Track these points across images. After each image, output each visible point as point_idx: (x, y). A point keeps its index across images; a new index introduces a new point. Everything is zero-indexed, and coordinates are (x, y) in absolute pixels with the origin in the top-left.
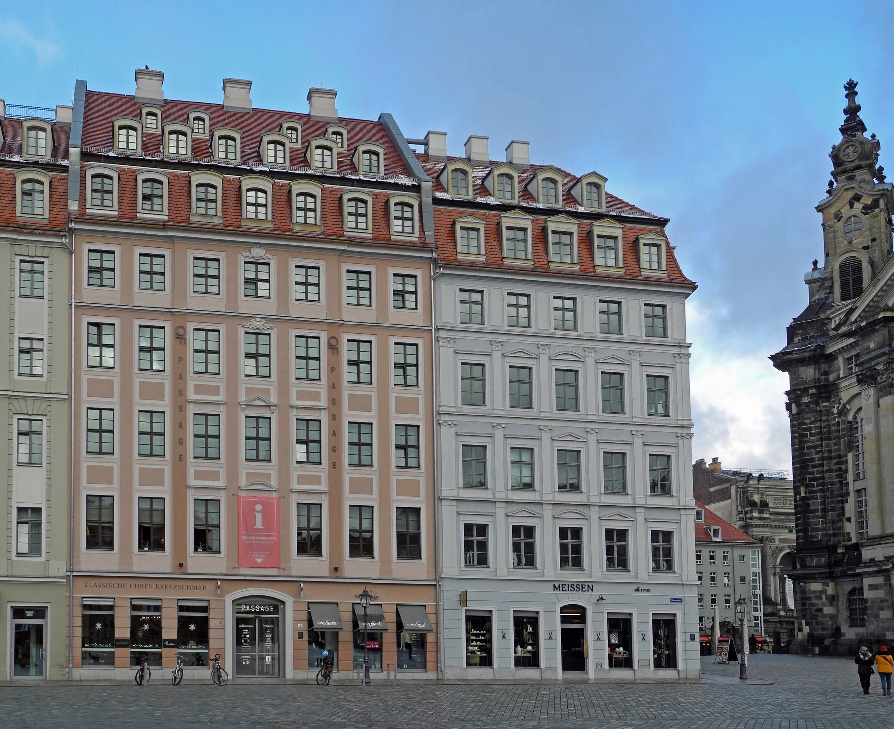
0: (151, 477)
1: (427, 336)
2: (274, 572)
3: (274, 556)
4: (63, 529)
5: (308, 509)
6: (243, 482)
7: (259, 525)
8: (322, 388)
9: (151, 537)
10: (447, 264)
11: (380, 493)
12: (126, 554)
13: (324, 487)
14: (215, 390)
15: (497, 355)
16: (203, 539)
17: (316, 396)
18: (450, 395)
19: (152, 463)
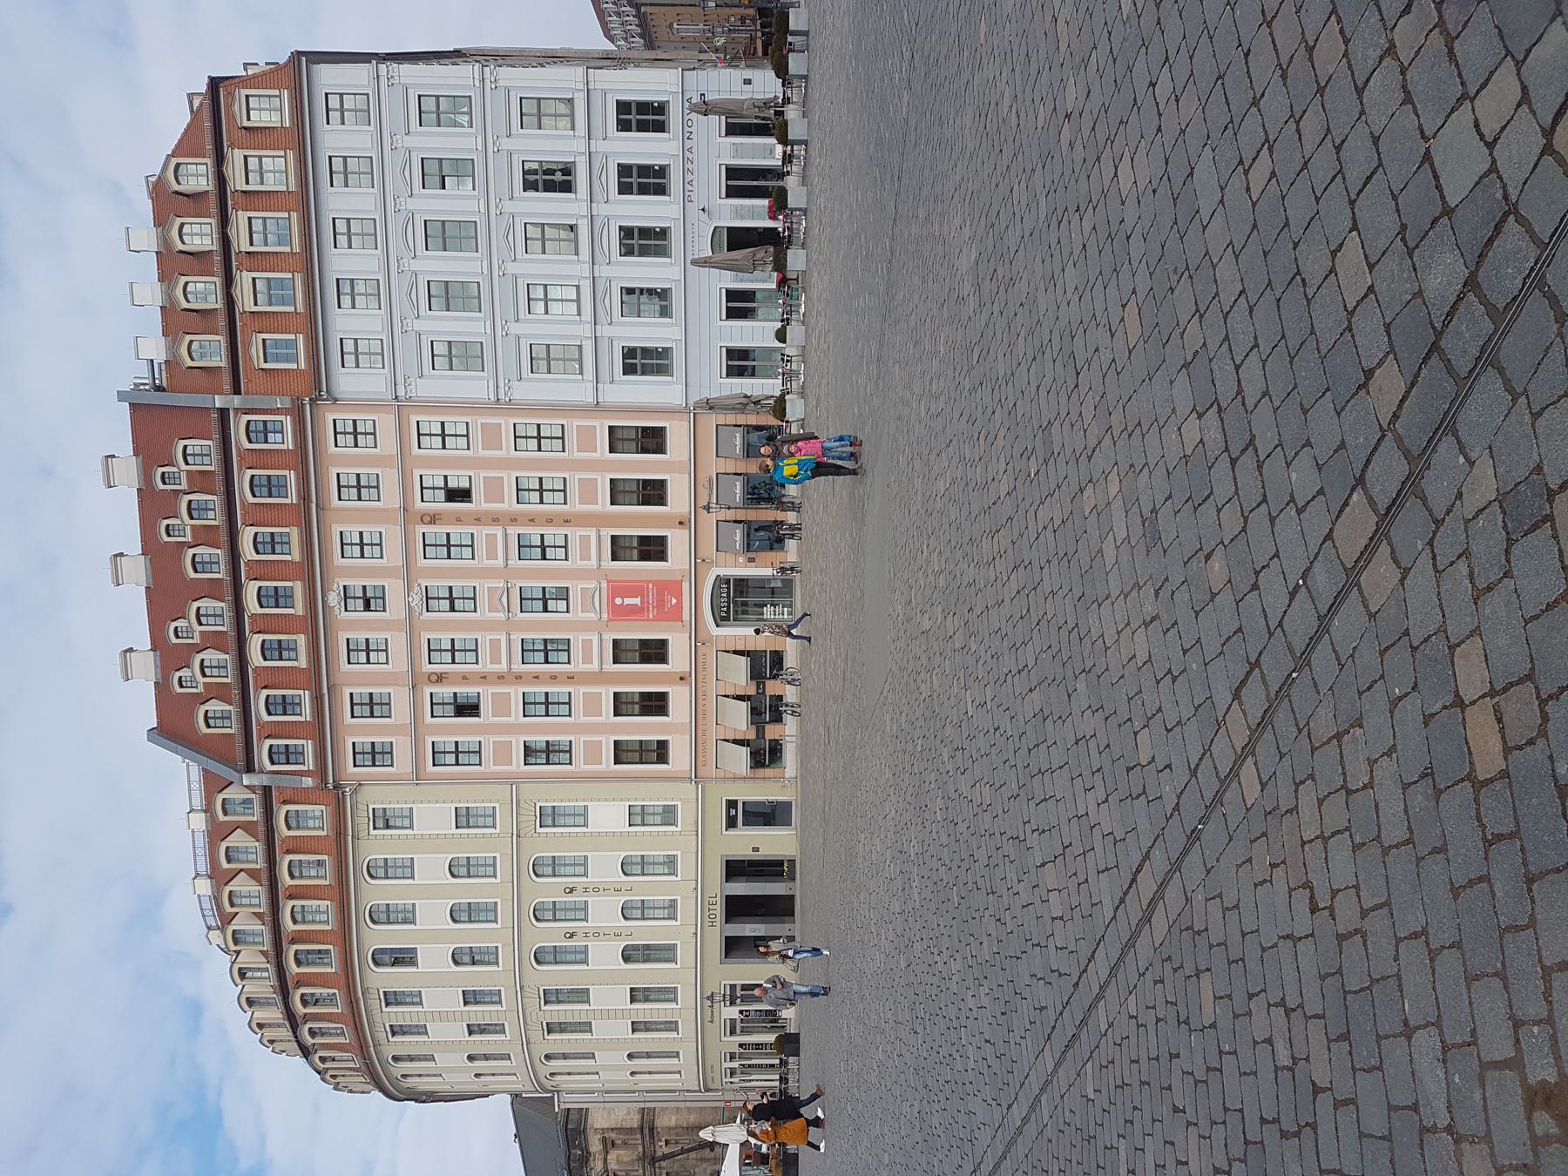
0: (592, 705)
1: (405, 411)
2: (686, 586)
4: (650, 786)
5: (618, 549)
6: (592, 616)
7: (637, 601)
8: (481, 532)
9: (655, 704)
10: (313, 388)
11: (594, 471)
12: (674, 728)
13: (592, 533)
14: (495, 644)
15: (418, 325)
16: (654, 652)
17: (491, 539)
18: (473, 386)
19: (578, 704)
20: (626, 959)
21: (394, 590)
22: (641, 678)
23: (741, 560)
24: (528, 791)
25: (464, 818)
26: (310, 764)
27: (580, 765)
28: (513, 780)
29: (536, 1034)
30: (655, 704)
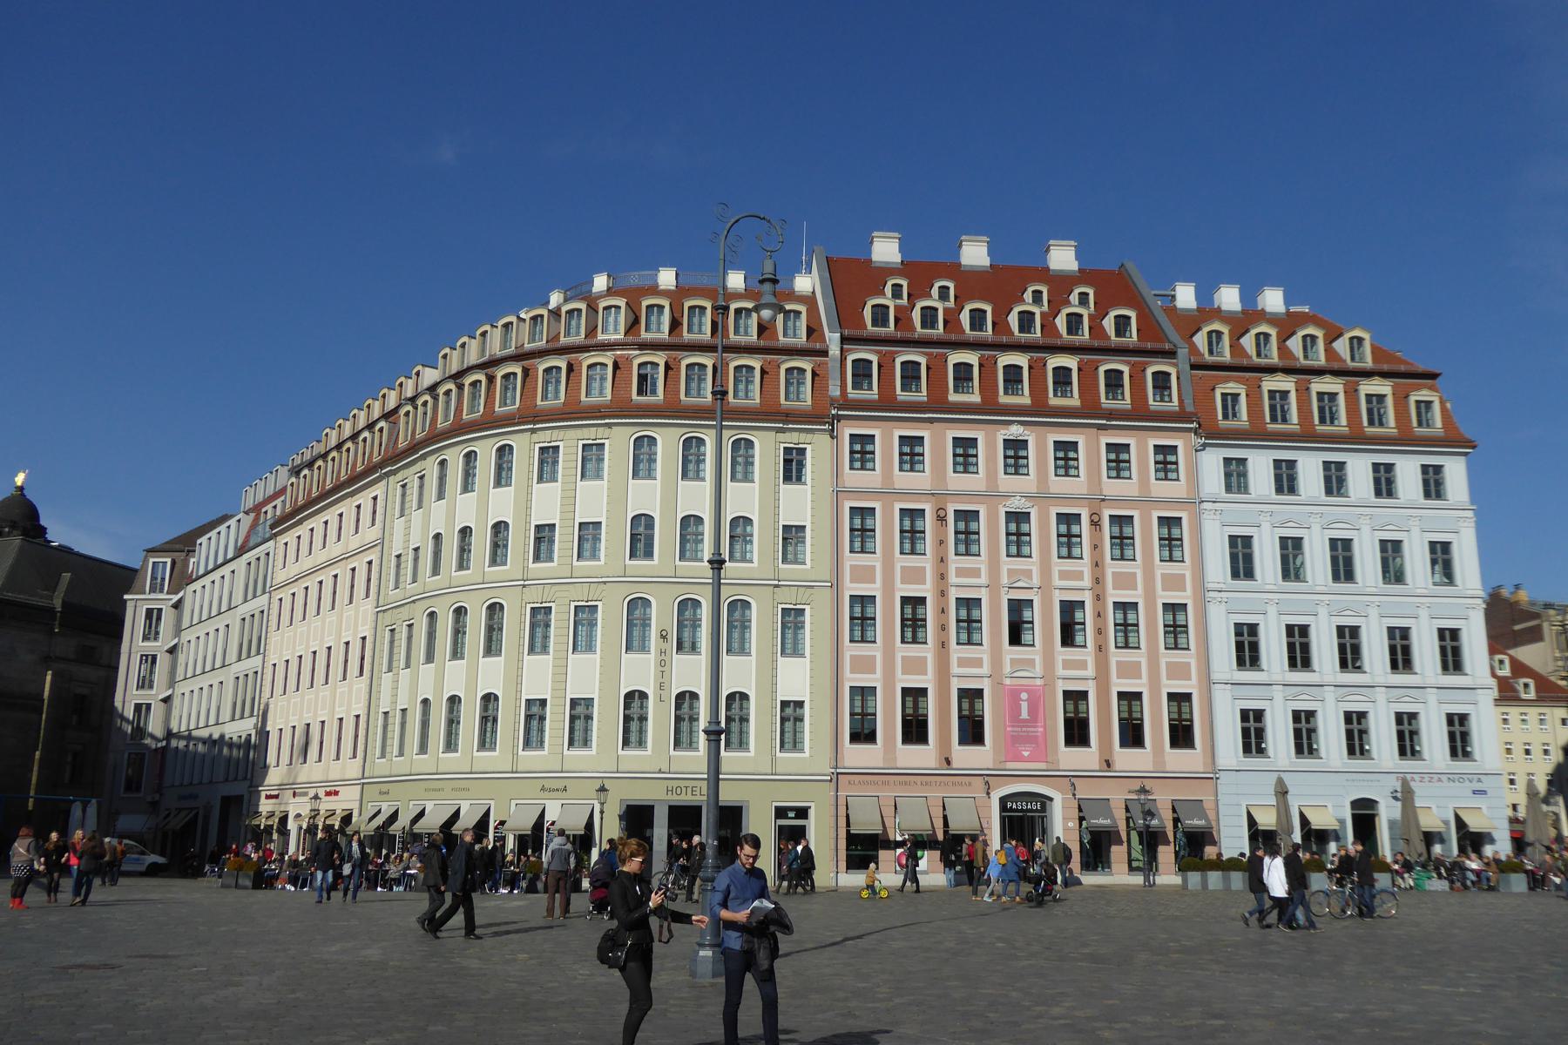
2: (1043, 766)
3: (1042, 749)
5: (1075, 698)
6: (1007, 669)
7: (1025, 715)
8: (1085, 566)
9: (915, 730)
12: (889, 748)
17: (1079, 576)
20: (630, 696)
21: (1026, 483)
22: (942, 717)
23: (1070, 824)
24: (824, 597)
25: (793, 535)
26: (853, 394)
27: (850, 650)
28: (836, 585)
29: (534, 597)
30: (915, 730)
